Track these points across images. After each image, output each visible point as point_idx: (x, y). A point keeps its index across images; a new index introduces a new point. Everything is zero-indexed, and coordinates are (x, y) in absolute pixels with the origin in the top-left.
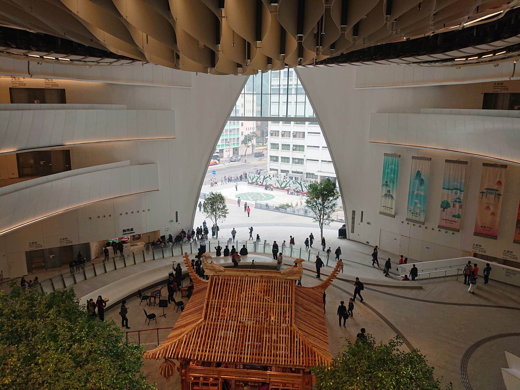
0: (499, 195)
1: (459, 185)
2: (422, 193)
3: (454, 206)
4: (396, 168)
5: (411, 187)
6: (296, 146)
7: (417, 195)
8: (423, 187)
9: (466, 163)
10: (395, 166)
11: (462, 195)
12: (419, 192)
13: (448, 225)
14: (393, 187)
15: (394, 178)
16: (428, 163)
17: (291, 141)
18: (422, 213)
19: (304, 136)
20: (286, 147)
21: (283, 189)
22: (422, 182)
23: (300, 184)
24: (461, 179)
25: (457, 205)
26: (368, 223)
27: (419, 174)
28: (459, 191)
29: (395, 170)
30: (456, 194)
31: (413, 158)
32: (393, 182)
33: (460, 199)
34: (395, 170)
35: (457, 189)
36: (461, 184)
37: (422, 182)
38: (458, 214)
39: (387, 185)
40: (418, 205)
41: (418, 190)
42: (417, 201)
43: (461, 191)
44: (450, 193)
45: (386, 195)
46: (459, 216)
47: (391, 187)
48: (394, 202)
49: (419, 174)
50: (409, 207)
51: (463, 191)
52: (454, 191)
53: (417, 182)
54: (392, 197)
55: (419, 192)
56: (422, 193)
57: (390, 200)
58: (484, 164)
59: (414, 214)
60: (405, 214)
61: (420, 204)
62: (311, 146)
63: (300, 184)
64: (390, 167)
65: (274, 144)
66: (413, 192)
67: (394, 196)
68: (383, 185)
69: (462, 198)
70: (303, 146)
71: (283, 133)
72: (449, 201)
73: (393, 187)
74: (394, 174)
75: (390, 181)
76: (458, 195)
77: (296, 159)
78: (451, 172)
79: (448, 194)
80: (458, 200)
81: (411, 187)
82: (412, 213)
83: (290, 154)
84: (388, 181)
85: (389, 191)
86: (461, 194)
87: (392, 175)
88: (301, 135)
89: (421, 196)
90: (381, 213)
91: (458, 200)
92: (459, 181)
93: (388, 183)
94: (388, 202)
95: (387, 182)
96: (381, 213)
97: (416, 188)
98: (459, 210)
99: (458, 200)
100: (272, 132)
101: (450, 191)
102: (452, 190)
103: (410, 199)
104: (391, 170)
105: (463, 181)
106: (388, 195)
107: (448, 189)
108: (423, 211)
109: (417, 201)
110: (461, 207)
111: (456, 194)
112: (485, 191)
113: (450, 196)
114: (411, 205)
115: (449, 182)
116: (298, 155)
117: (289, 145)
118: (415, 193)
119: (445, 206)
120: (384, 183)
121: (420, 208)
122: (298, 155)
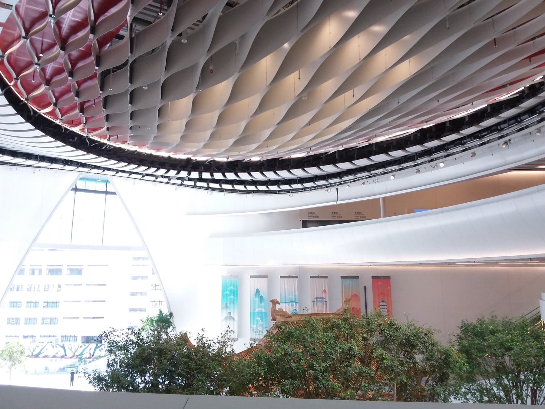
4: (235, 289)
8: (263, 304)
9: (296, 277)
15: (234, 299)
16: (265, 280)
21: (37, 356)
23: (63, 347)
24: (295, 292)
27: (258, 291)
28: (294, 303)
30: (292, 306)
31: (251, 277)
32: (234, 303)
33: (296, 310)
35: (292, 301)
39: (227, 307)
40: (261, 323)
43: (296, 303)
48: (236, 324)
49: (258, 291)
50: (252, 326)
52: (291, 303)
53: (257, 299)
54: (234, 319)
57: (232, 322)
61: (262, 321)
63: (63, 347)
67: (236, 318)
68: (223, 308)
69: (298, 310)
74: (234, 296)
75: (230, 303)
77: (46, 319)
82: (256, 332)
83: (40, 313)
85: (230, 314)
86: (296, 305)
87: (232, 296)
89: (262, 313)
101: (287, 304)
102: (289, 303)
103: (252, 319)
104: (230, 291)
105: (297, 293)
106: (230, 317)
107: (285, 302)
111: (292, 306)
112: (315, 300)
114: (254, 324)
116: (50, 313)
118: (257, 311)
121: (262, 325)
122: (50, 313)
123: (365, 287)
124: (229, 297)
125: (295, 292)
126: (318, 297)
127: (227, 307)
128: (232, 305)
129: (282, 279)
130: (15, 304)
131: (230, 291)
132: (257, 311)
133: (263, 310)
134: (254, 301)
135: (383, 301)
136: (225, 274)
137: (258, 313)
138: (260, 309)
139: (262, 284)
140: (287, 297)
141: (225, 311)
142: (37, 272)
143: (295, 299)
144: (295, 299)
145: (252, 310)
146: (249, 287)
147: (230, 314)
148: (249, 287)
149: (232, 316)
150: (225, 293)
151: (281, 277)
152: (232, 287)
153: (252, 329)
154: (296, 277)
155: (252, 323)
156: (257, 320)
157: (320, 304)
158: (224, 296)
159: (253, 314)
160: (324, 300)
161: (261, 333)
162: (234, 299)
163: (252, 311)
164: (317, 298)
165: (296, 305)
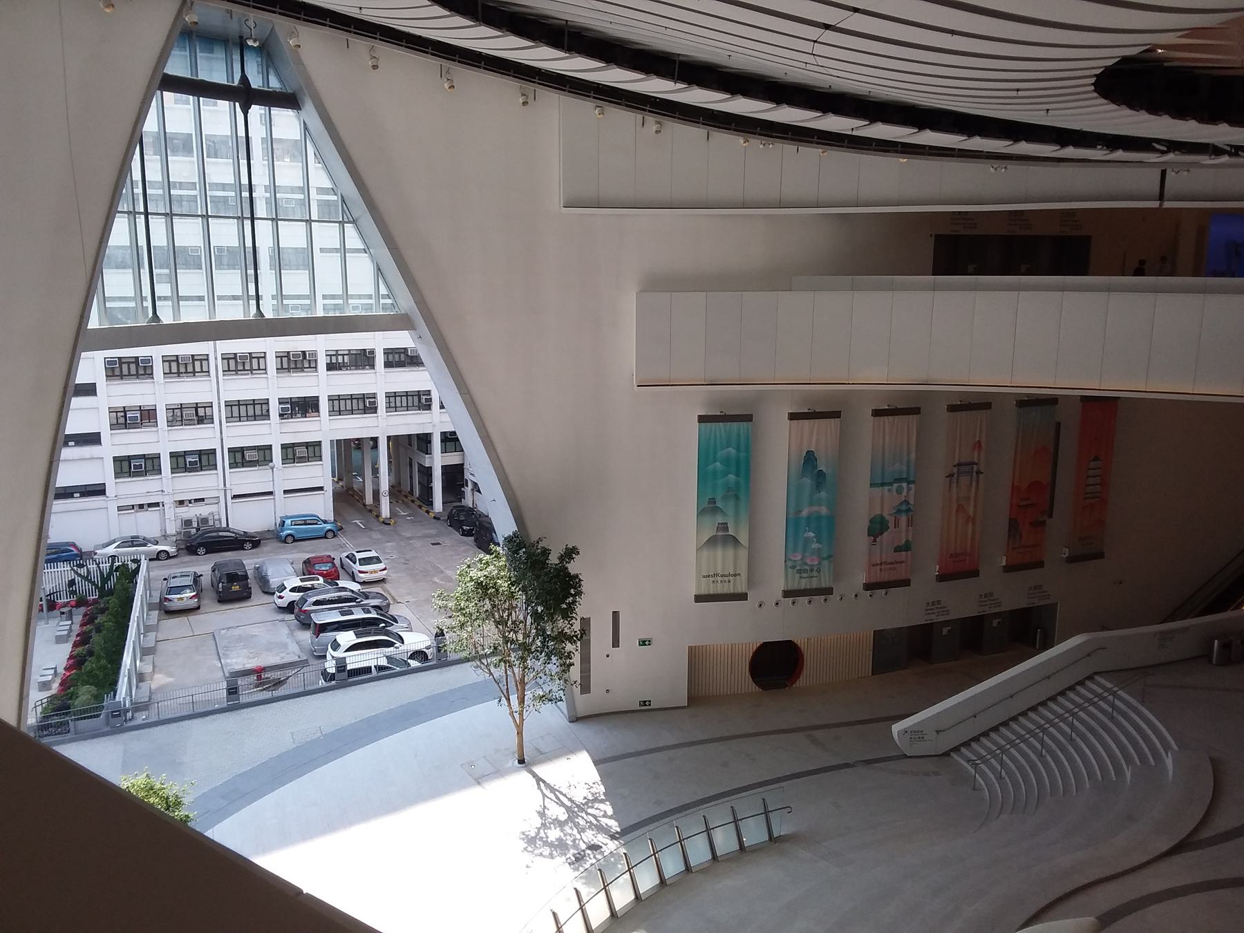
0: (979, 473)
1: (905, 468)
3: (896, 525)
4: (742, 455)
8: (823, 494)
10: (738, 449)
11: (912, 492)
13: (886, 577)
14: (737, 513)
18: (825, 563)
22: (820, 479)
24: (909, 454)
25: (903, 519)
26: (643, 643)
28: (904, 485)
30: (899, 492)
32: (737, 497)
33: (907, 502)
35: (899, 480)
36: (908, 467)
37: (820, 479)
38: (907, 541)
40: (815, 546)
44: (886, 493)
45: (712, 542)
46: (907, 547)
47: (730, 511)
48: (743, 554)
49: (810, 458)
51: (913, 482)
52: (895, 485)
53: (808, 481)
54: (735, 541)
55: (815, 508)
57: (730, 552)
58: (952, 408)
59: (805, 571)
60: (776, 579)
64: (720, 454)
67: (743, 538)
69: (912, 502)
72: (887, 517)
73: (737, 513)
74: (737, 475)
75: (725, 498)
76: (905, 493)
78: (887, 437)
79: (882, 498)
82: (799, 572)
85: (724, 527)
87: (732, 477)
90: (699, 599)
92: (905, 461)
93: (719, 504)
94: (723, 558)
95: (713, 501)
96: (699, 599)
98: (907, 531)
99: (905, 508)
101: (886, 488)
102: (890, 484)
104: (726, 461)
105: (913, 456)
107: (883, 484)
108: (830, 556)
109: (811, 534)
110: (910, 523)
111: (899, 492)
112: (955, 470)
113: (886, 501)
114: (795, 551)
115: (883, 468)
118: (805, 513)
119: (877, 528)
120: (706, 505)
123: (1058, 425)
124: (720, 481)
125: (909, 454)
126: (963, 460)
128: (732, 503)
131: (726, 461)
132: (805, 513)
133: (824, 510)
135: (1096, 459)
137: (808, 518)
138: (815, 508)
139: (820, 435)
145: (792, 511)
146: (779, 446)
147: (727, 529)
148: (779, 446)
149: (731, 532)
150: (710, 467)
151: (877, 413)
152: (732, 451)
153: (790, 564)
155: (791, 545)
156: (807, 541)
157: (964, 480)
158: (705, 476)
159: (794, 524)
160: (975, 467)
161: (815, 574)
163: (791, 516)
164: (959, 465)
165: (909, 489)
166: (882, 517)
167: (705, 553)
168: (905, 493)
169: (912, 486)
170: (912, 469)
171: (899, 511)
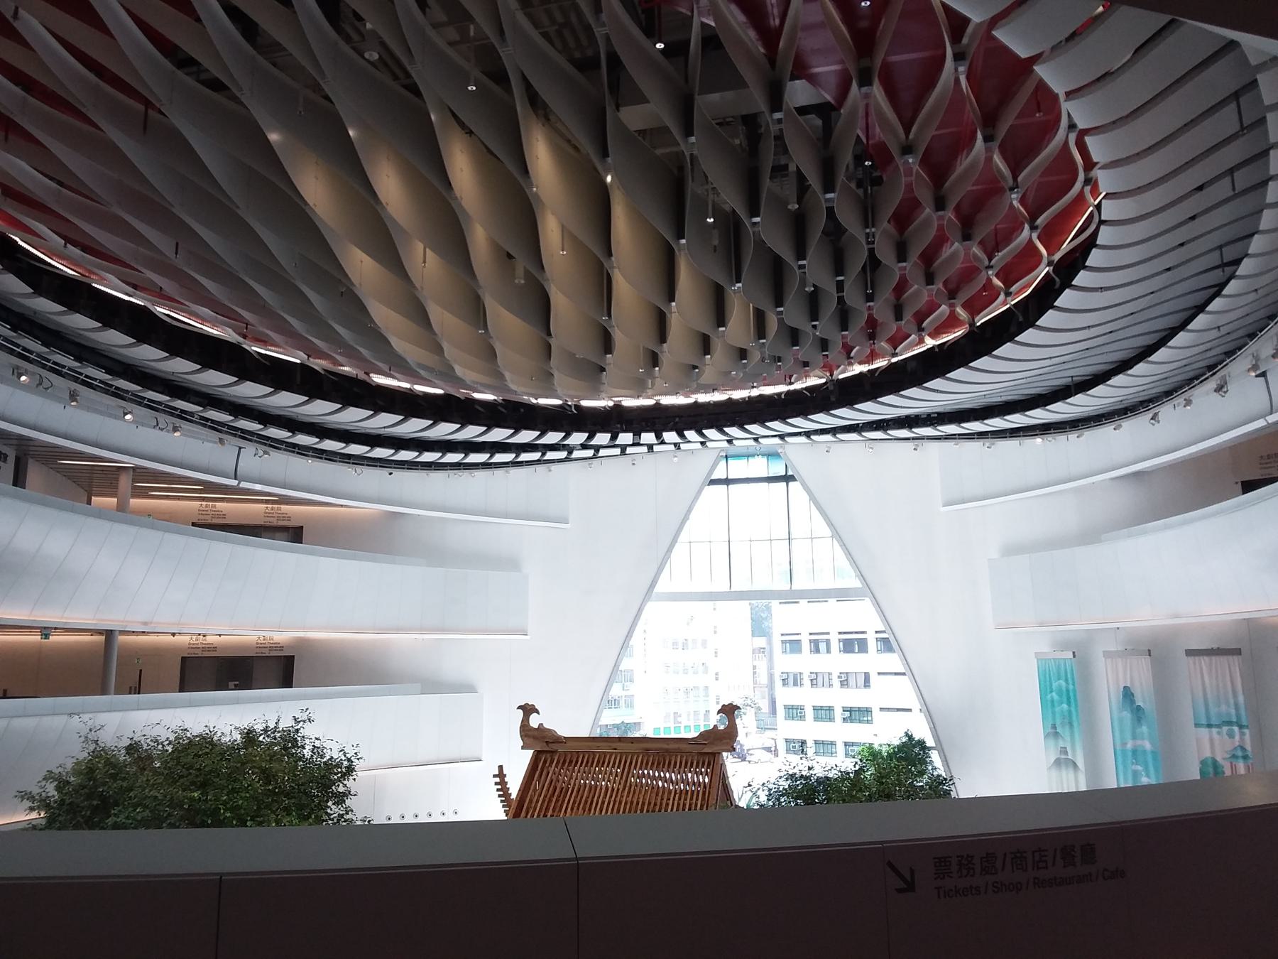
1: (1233, 712)
2: (1148, 746)
4: (1071, 687)
5: (1117, 728)
6: (850, 710)
7: (1134, 752)
8: (1144, 729)
9: (1237, 652)
11: (1247, 737)
12: (1139, 742)
15: (1070, 712)
17: (839, 698)
19: (867, 683)
20: (824, 713)
27: (1128, 694)
28: (1236, 729)
29: (1068, 691)
30: (1231, 735)
32: (1071, 724)
33: (1243, 748)
34: (1068, 691)
35: (1229, 723)
37: (1138, 713)
39: (1056, 735)
41: (1134, 737)
42: (1139, 768)
43: (1241, 727)
44: (1216, 736)
45: (1058, 763)
47: (1068, 739)
49: (1128, 694)
52: (1225, 729)
53: (1127, 715)
54: (1075, 765)
55: (1139, 742)
56: (1148, 746)
61: (1148, 776)
62: (889, 709)
64: (1055, 685)
65: (792, 707)
66: (1124, 744)
67: (1080, 763)
68: (1047, 736)
69: (1248, 747)
70: (868, 711)
71: (814, 676)
74: (1069, 704)
75: (1063, 724)
79: (1211, 740)
80: (1240, 753)
81: (1117, 728)
84: (1058, 722)
85: (1064, 751)
87: (1065, 706)
88: (861, 680)
89: (1144, 752)
91: (1240, 753)
92: (1232, 701)
95: (1054, 727)
97: (1128, 735)
100: (785, 676)
101: (1214, 730)
102: (1218, 726)
103: (1121, 767)
104: (1060, 693)
105: (1241, 699)
107: (1209, 726)
109: (1139, 768)
111: (1231, 735)
117: (830, 709)
127: (1056, 735)
128: (1067, 728)
129: (1191, 659)
130: (795, 712)
132: (1129, 746)
134: (1121, 720)
136: (1045, 648)
140: (1213, 711)
141: (1051, 742)
142: (822, 646)
143: (1238, 716)
144: (1238, 716)
146: (1107, 682)
147: (1066, 753)
148: (1107, 682)
151: (1190, 653)
152: (1062, 682)
154: (1237, 652)
158: (1047, 705)
162: (1070, 712)
165: (1242, 734)
166: (1215, 762)
167: (1054, 773)
168: (1237, 738)
169: (1246, 731)
170: (1243, 712)
171: (1234, 756)
